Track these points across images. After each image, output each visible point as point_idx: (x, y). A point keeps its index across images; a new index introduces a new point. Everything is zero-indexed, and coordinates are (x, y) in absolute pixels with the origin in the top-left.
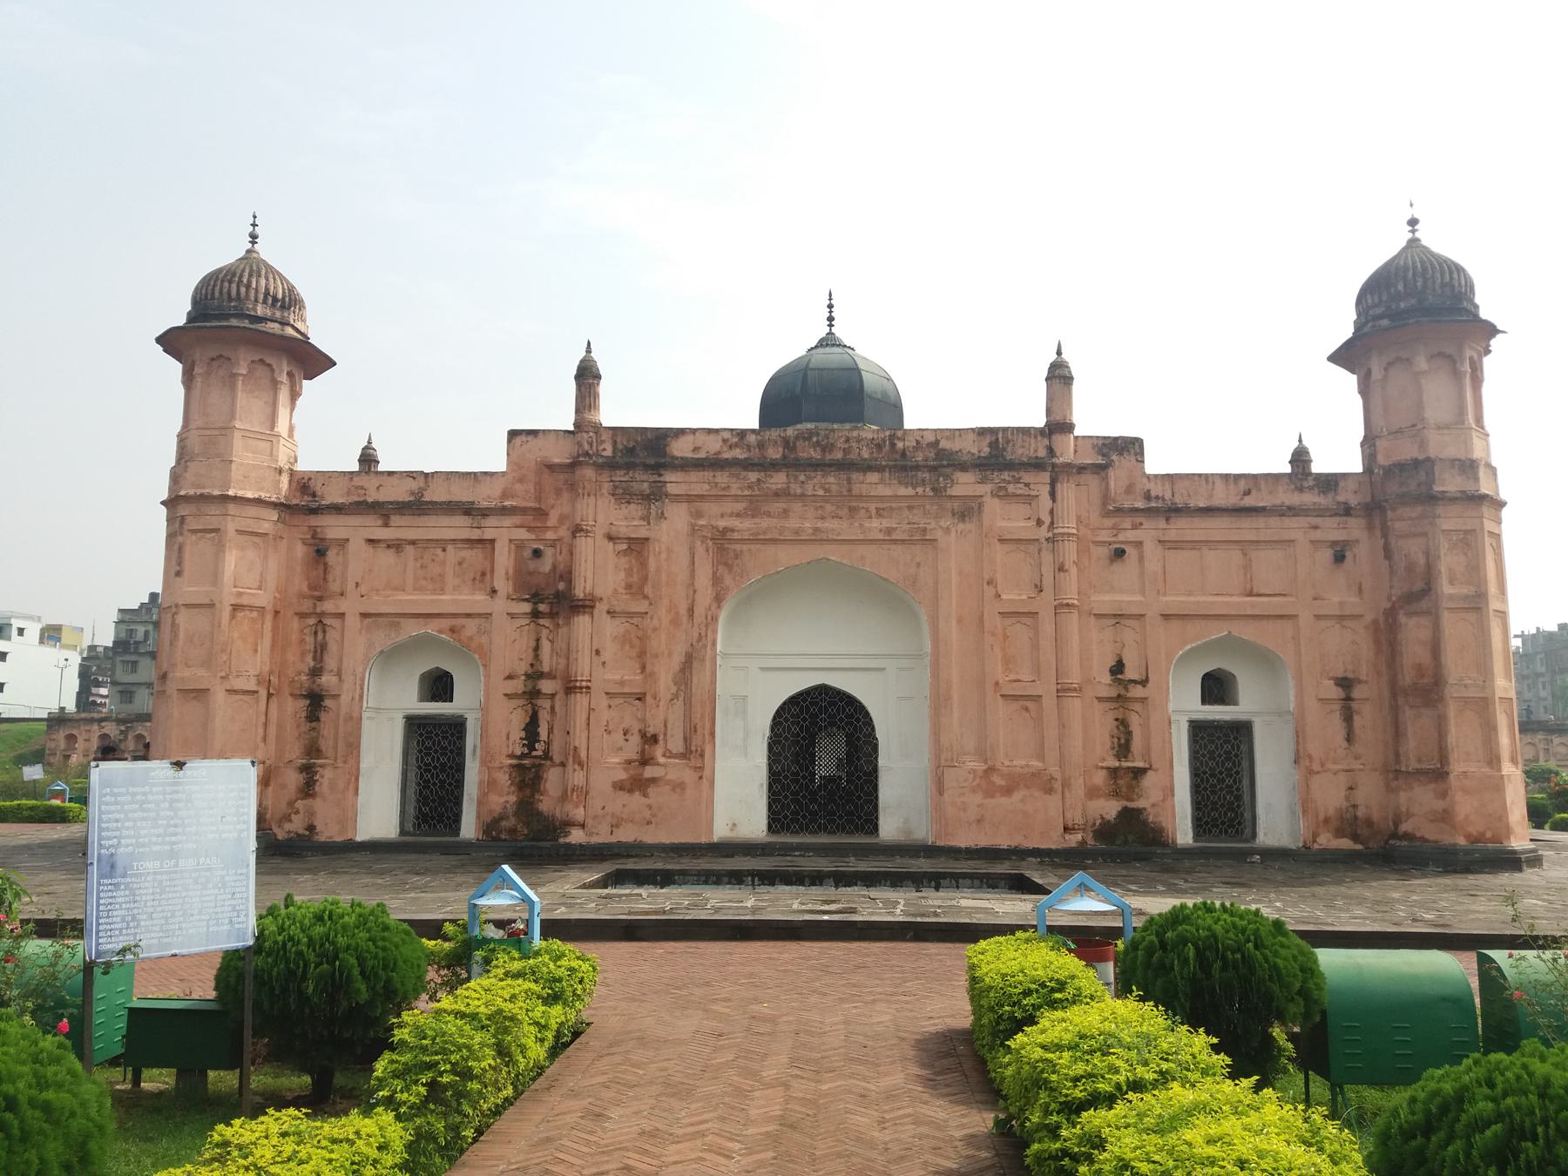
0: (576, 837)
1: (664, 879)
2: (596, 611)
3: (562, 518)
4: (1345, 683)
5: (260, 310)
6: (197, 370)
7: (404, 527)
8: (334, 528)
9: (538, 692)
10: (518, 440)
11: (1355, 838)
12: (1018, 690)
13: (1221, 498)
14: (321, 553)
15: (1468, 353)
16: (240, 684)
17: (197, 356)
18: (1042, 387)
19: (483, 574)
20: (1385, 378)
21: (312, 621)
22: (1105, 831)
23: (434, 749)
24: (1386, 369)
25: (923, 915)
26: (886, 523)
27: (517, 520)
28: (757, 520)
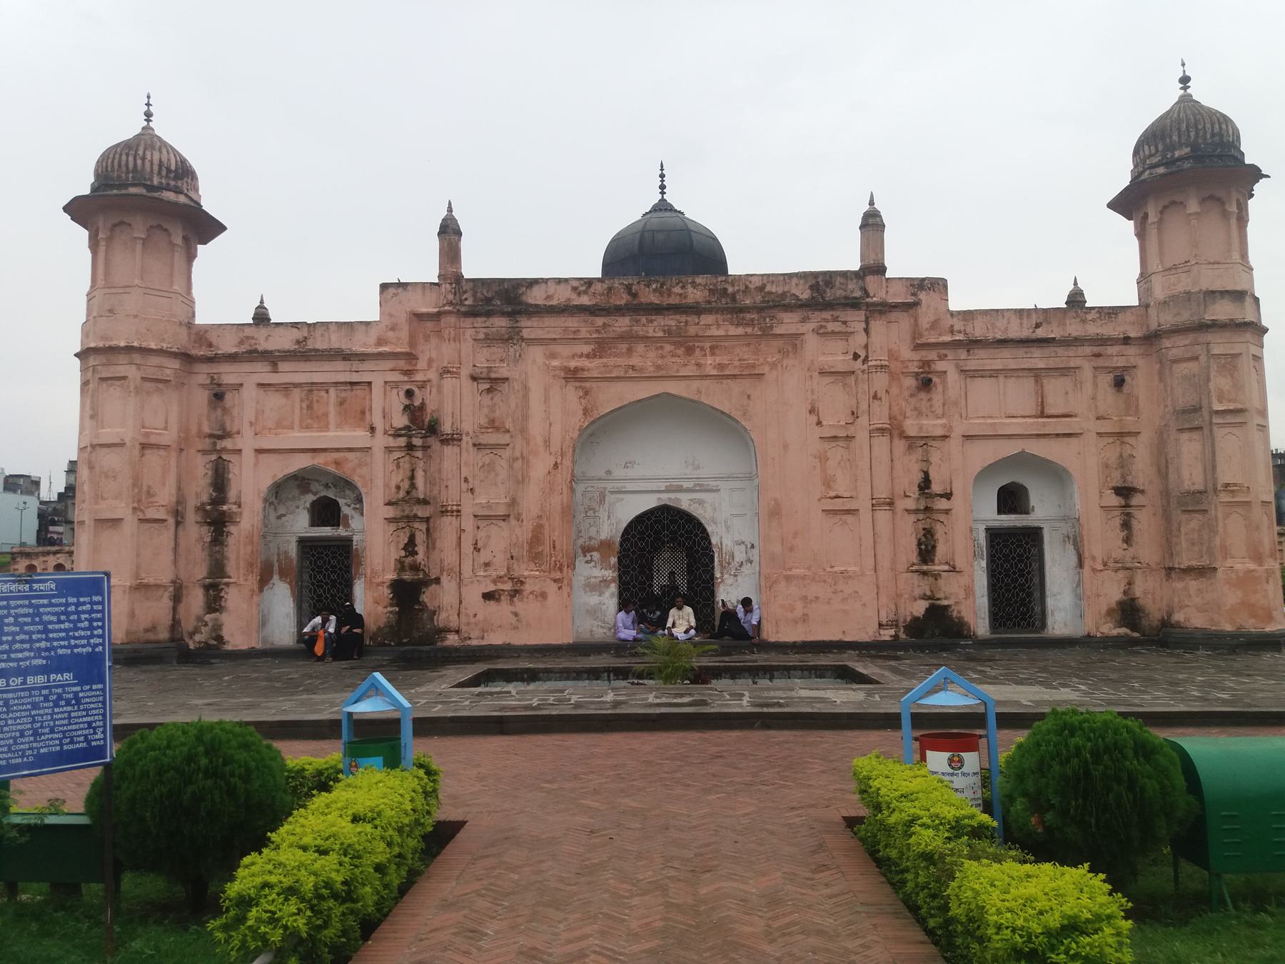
0: (452, 640)
1: (532, 676)
2: (464, 443)
3: (430, 361)
4: (1125, 492)
5: (156, 181)
6: (101, 235)
7: (292, 373)
8: (229, 374)
9: (416, 513)
10: (392, 291)
11: (1134, 627)
12: (838, 504)
13: (1015, 332)
14: (219, 397)
15: (1235, 196)
16: (152, 513)
17: (101, 224)
18: (857, 234)
19: (363, 412)
20: (1160, 222)
21: (214, 457)
22: (915, 627)
24: (1161, 212)
25: (767, 705)
26: (718, 360)
27: (390, 364)
28: (605, 360)
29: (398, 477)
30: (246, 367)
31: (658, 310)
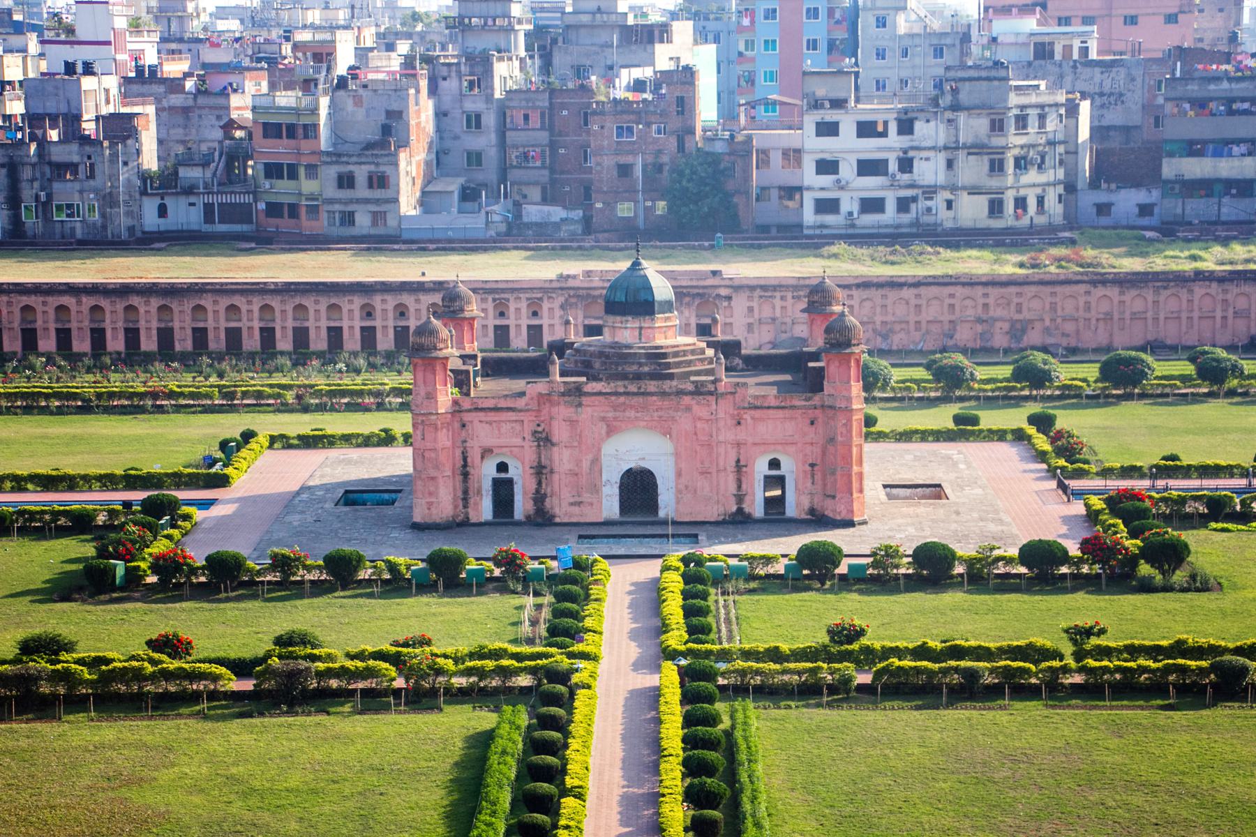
0: (557, 520)
4: (812, 465)
8: (467, 417)
9: (540, 471)
14: (464, 426)
23: (503, 491)
29: (534, 457)
30: (474, 414)
31: (634, 394)
